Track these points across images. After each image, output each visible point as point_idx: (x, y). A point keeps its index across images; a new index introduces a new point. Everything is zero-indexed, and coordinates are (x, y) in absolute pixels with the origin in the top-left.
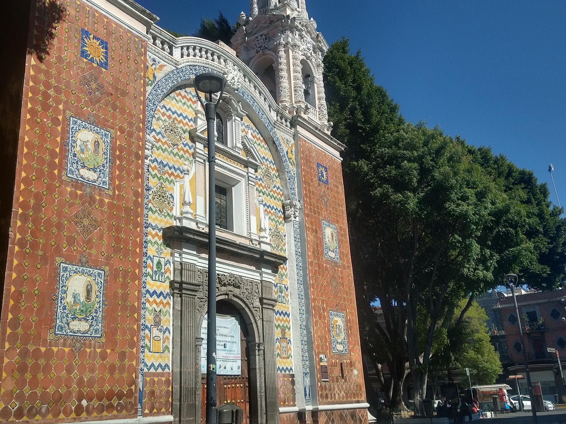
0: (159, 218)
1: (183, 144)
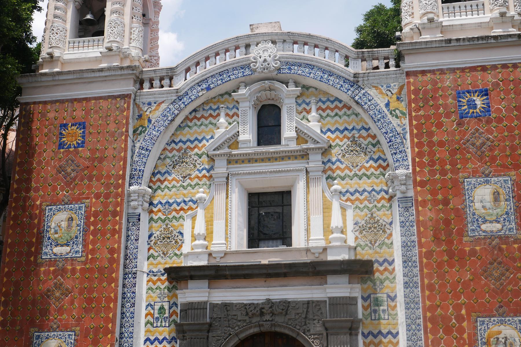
0: (163, 261)
1: (198, 170)
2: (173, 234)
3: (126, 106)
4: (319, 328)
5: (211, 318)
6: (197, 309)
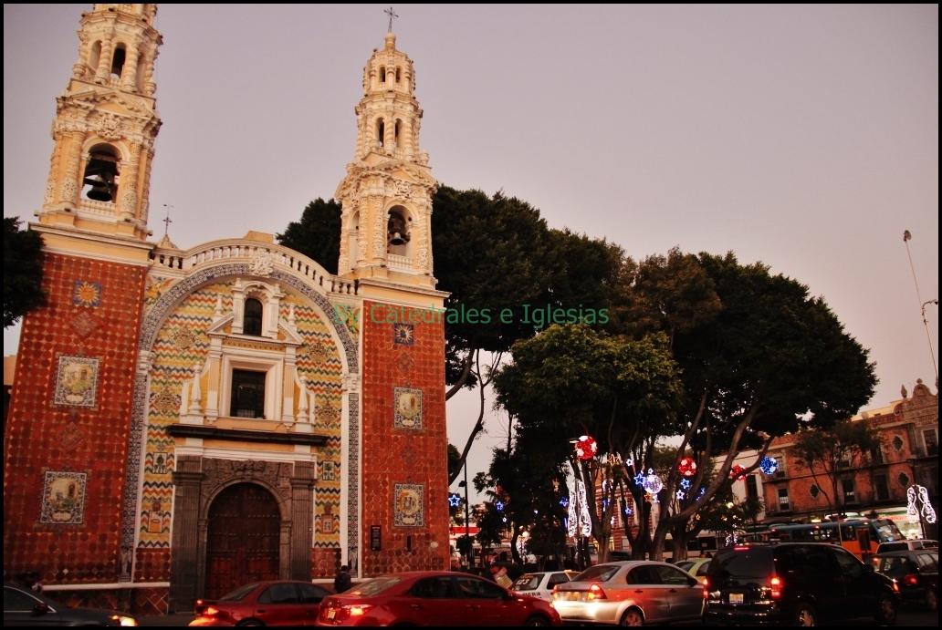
4: (287, 483)
5: (203, 469)
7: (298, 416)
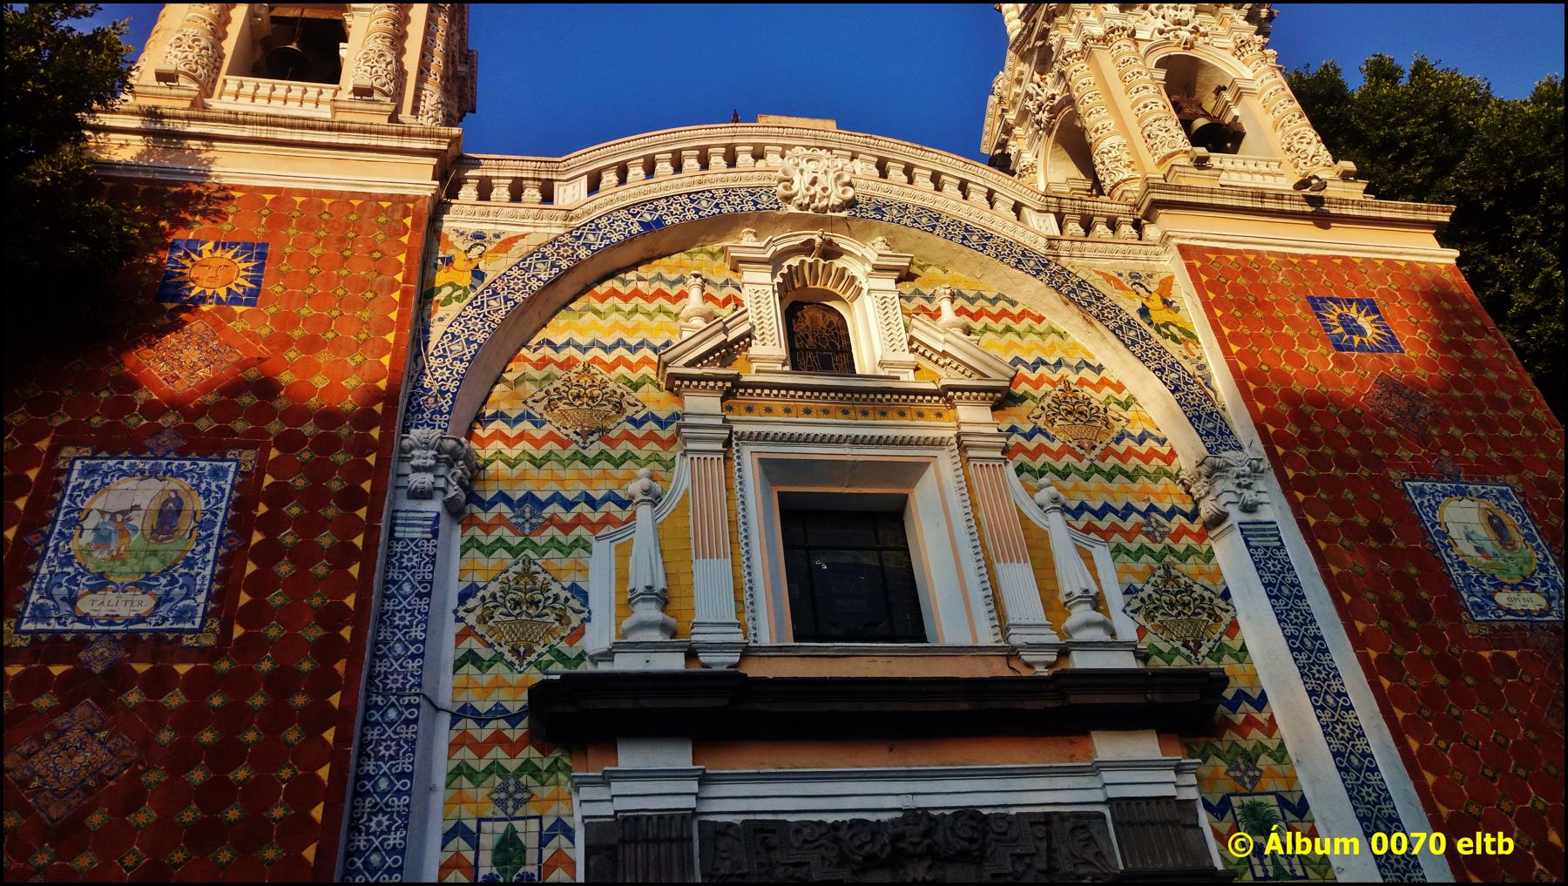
0: (514, 678)
1: (631, 420)
2: (550, 594)
3: (408, 221)
6: (657, 841)
7: (1070, 622)
